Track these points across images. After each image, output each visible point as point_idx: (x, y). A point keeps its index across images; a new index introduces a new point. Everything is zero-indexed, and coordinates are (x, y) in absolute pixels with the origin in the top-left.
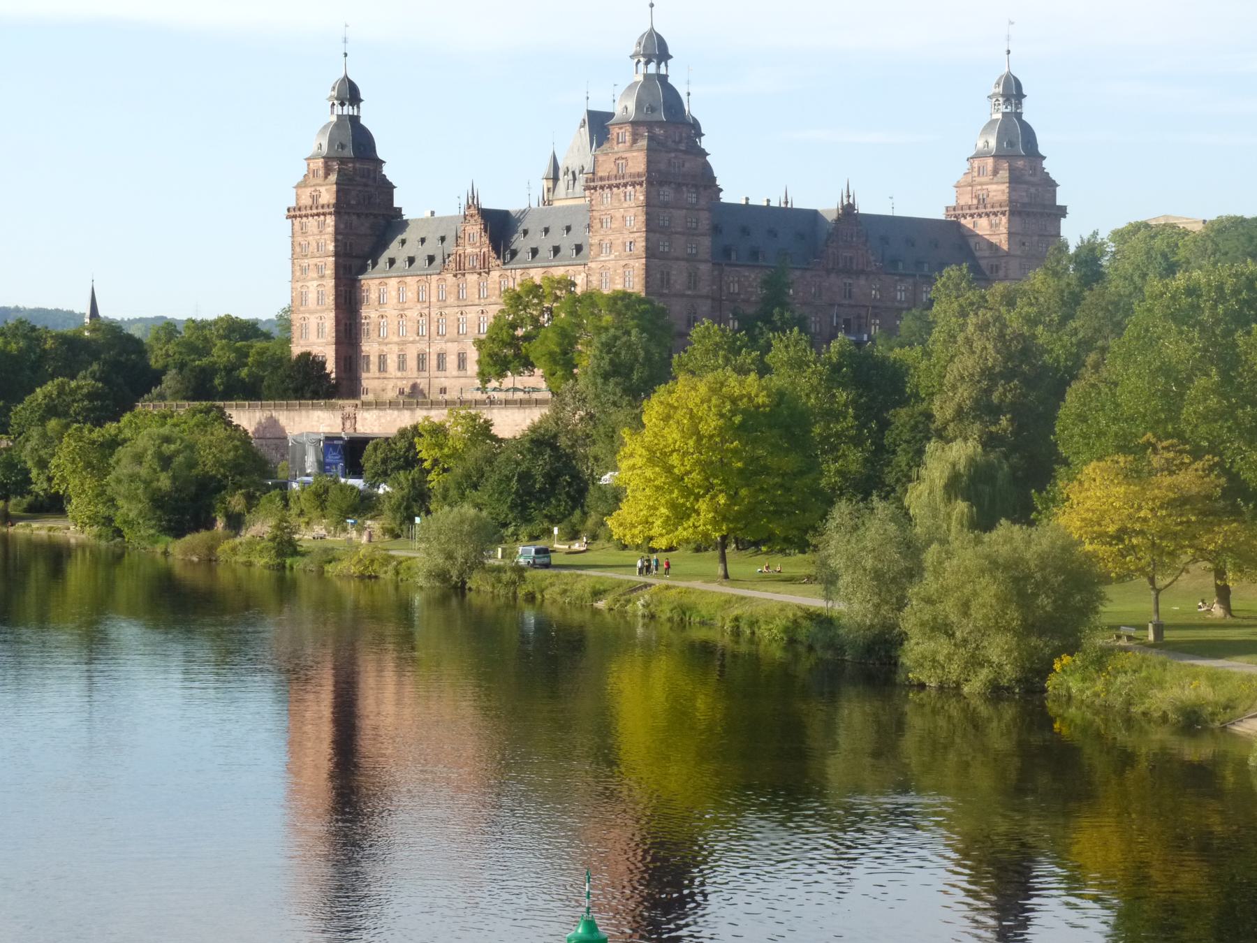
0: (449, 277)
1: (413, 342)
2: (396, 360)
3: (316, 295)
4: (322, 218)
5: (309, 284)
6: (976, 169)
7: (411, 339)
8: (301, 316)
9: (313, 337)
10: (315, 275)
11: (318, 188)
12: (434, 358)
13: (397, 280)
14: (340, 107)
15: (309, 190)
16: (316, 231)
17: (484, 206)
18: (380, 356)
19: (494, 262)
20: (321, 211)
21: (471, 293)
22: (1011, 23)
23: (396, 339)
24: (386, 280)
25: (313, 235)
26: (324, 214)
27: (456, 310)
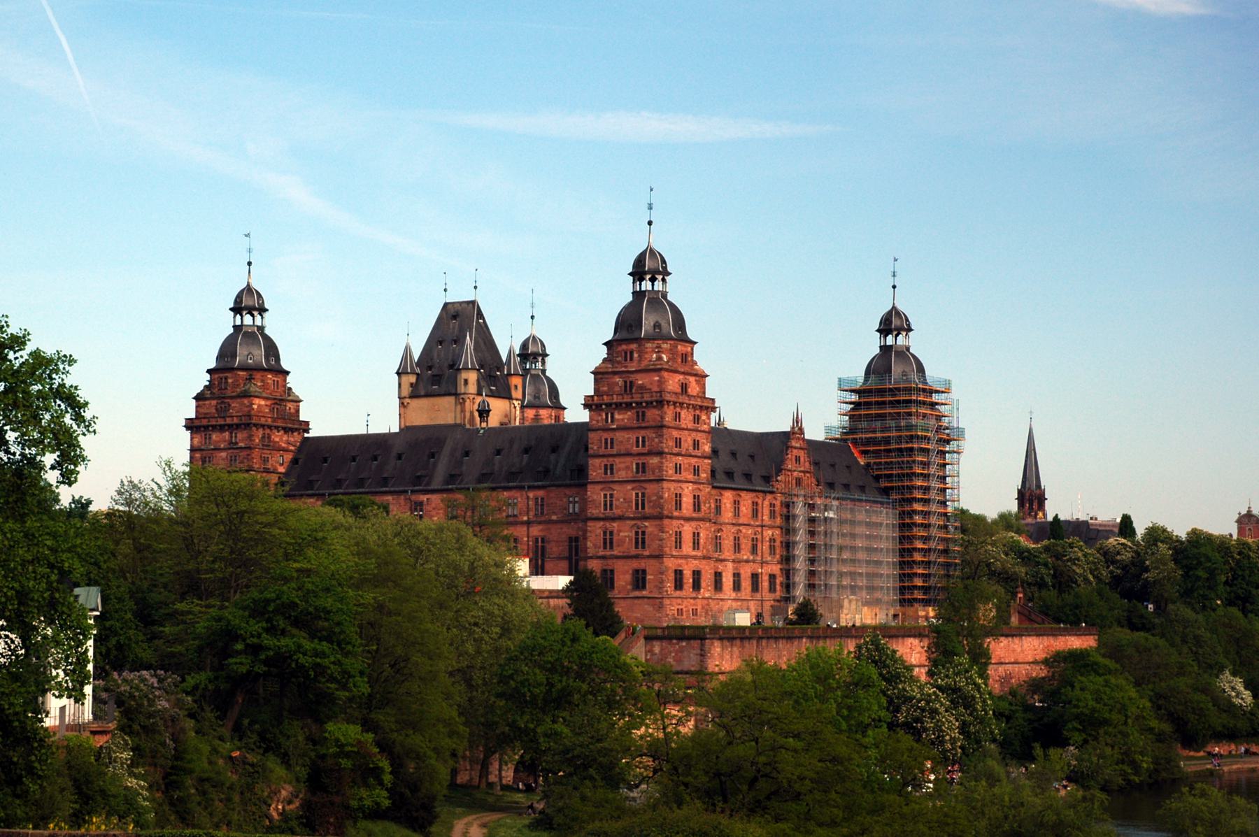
1: (747, 561)
2: (731, 579)
3: (691, 500)
5: (684, 485)
6: (553, 417)
7: (745, 557)
8: (675, 522)
9: (687, 548)
11: (688, 377)
12: (766, 578)
13: (734, 493)
14: (649, 284)
17: (732, 424)
18: (716, 573)
19: (817, 490)
20: (686, 400)
24: (723, 492)
25: (687, 429)
26: (701, 407)
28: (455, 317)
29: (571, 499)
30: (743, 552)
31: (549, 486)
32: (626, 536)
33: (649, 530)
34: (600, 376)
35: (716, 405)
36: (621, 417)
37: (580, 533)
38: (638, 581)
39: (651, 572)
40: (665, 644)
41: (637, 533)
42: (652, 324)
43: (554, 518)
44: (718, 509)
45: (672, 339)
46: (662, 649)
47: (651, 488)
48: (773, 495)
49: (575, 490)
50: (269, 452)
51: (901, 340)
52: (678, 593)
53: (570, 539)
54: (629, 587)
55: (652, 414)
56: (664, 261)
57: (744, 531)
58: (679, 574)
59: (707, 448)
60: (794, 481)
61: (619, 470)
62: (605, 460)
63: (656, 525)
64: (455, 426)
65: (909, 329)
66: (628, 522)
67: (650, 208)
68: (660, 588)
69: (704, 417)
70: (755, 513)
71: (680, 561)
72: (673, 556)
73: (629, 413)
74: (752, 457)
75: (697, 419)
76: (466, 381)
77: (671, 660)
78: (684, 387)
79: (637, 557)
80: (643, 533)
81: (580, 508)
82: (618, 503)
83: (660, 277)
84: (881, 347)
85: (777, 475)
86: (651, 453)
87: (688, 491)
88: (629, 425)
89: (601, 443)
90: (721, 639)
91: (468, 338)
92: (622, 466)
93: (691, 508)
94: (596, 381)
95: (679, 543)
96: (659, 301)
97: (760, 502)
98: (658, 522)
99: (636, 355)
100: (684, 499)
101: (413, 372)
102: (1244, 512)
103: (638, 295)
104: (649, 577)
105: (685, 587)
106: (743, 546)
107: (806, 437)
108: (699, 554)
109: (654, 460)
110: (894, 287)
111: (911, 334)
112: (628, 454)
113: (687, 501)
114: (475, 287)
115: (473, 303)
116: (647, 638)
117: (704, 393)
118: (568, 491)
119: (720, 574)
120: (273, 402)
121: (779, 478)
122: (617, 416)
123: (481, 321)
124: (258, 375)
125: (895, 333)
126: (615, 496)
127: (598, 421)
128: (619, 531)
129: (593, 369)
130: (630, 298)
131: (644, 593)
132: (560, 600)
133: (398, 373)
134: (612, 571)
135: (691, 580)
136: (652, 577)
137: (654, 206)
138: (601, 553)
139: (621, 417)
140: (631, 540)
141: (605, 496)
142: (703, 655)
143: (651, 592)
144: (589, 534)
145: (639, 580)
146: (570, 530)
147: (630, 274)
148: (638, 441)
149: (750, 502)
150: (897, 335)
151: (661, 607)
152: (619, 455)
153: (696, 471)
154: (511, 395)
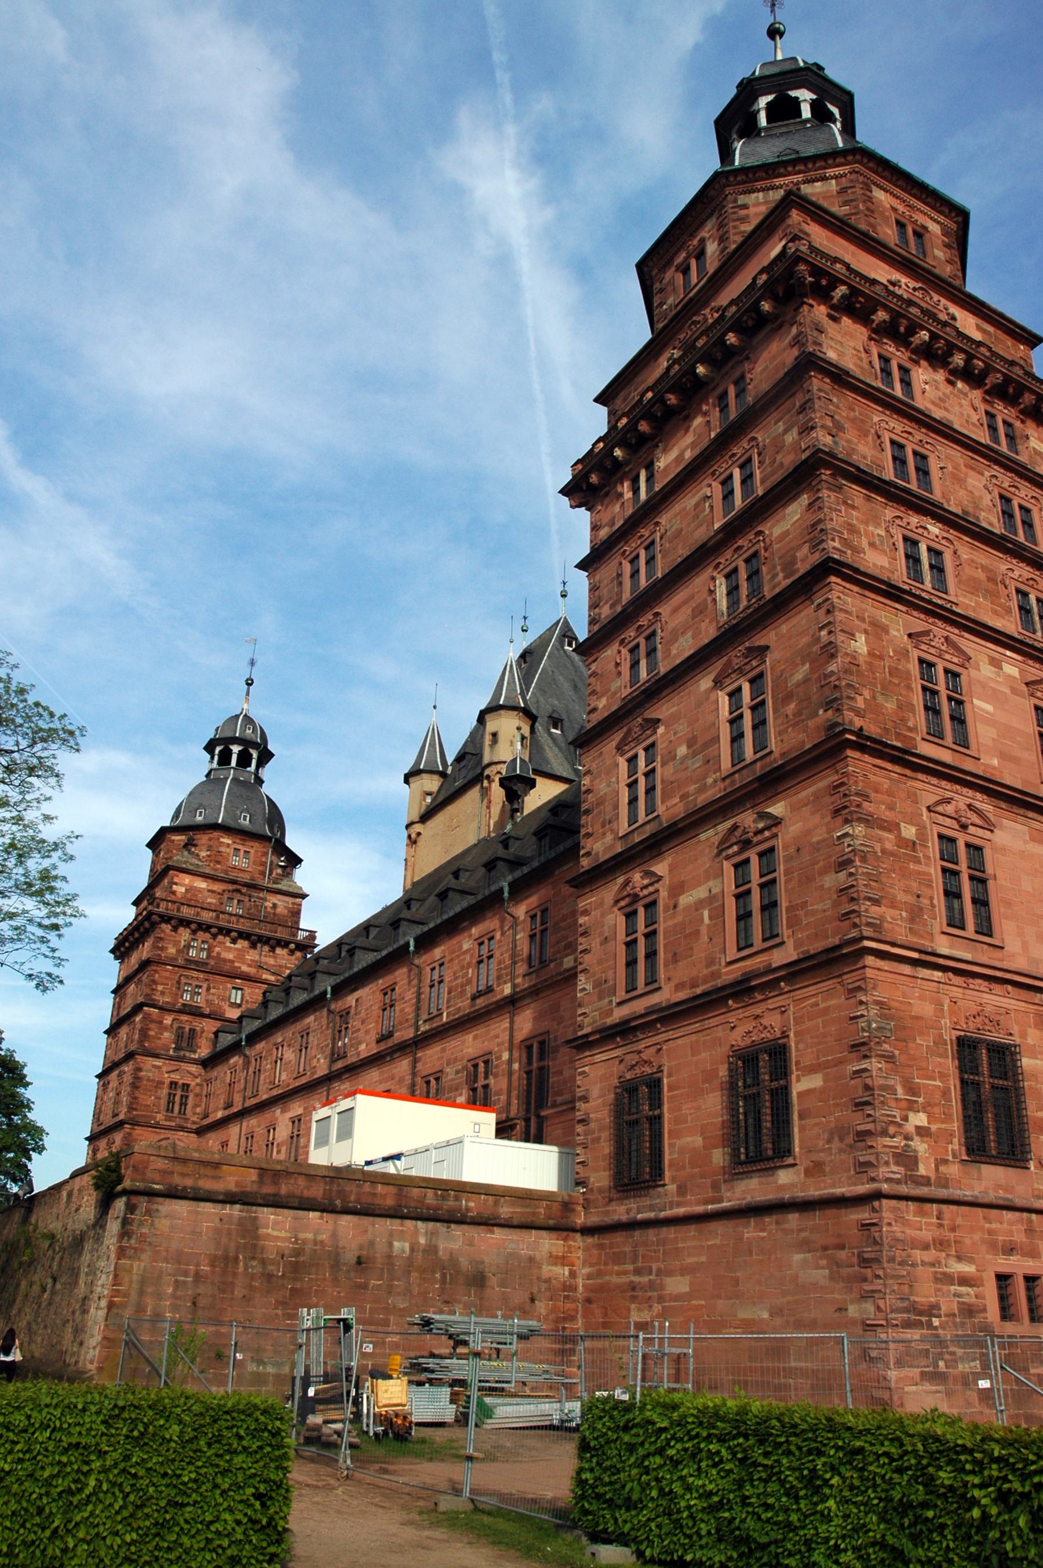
32: (700, 904)
36: (673, 454)
39: (808, 1060)
50: (201, 976)
54: (719, 1157)
63: (817, 797)
66: (711, 835)
68: (862, 1136)
72: (928, 961)
73: (698, 421)
89: (620, 584)
104: (801, 1085)
120: (231, 887)
124: (203, 839)
126: (661, 746)
128: (678, 889)
132: (346, 1221)
134: (654, 1085)
136: (814, 1082)
140: (718, 914)
143: (815, 1170)
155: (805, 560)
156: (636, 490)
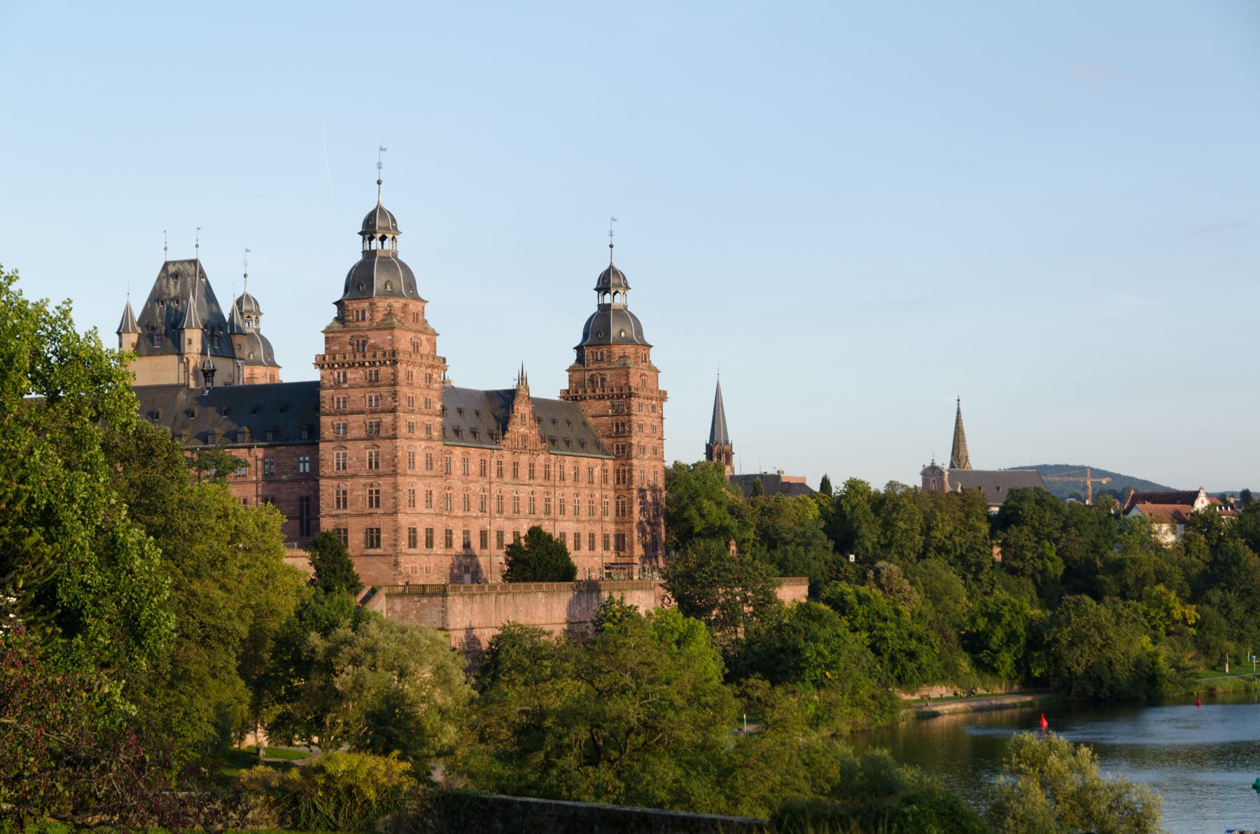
0: (507, 457)
2: (462, 536)
4: (429, 371)
5: (417, 443)
7: (474, 515)
8: (408, 480)
9: (421, 506)
10: (423, 435)
11: (419, 335)
12: (494, 535)
15: (410, 335)
16: (423, 384)
17: (458, 383)
19: (540, 446)
21: (524, 472)
22: (248, 251)
23: (460, 513)
27: (511, 488)
28: (176, 276)
29: (301, 459)
30: (472, 509)
31: (279, 445)
33: (382, 489)
34: (331, 335)
35: (447, 363)
37: (311, 493)
38: (372, 540)
40: (406, 601)
41: (371, 492)
42: (383, 283)
43: (284, 477)
44: (448, 465)
45: (403, 296)
46: (403, 607)
47: (385, 446)
48: (500, 452)
49: (305, 449)
51: (619, 301)
52: (412, 551)
53: (301, 499)
54: (363, 546)
55: (385, 371)
56: (394, 220)
57: (473, 488)
58: (413, 531)
59: (438, 407)
60: (520, 439)
61: (353, 429)
62: (337, 418)
64: (184, 385)
65: (627, 288)
66: (362, 481)
67: (380, 168)
69: (435, 376)
70: (483, 473)
71: (414, 519)
74: (477, 414)
75: (429, 378)
76: (190, 342)
77: (413, 618)
78: (416, 346)
79: (370, 514)
80: (377, 492)
81: (310, 467)
82: (350, 462)
83: (390, 236)
84: (599, 305)
85: (504, 434)
86: (383, 411)
87: (420, 449)
88: (361, 384)
90: (462, 595)
91: (191, 297)
92: (356, 425)
93: (424, 466)
94: (327, 338)
95: (412, 503)
96: (391, 263)
97: (488, 459)
98: (391, 480)
99: (367, 314)
100: (417, 458)
101: (134, 331)
102: (928, 464)
103: (369, 255)
104: (382, 536)
105: (419, 544)
106: (472, 504)
107: (532, 395)
108: (431, 511)
109: (387, 419)
110: (611, 246)
111: (628, 292)
112: (362, 412)
113: (420, 460)
114: (197, 246)
115: (195, 262)
116: (388, 595)
117: (435, 351)
118: (297, 450)
119: (450, 532)
121: (506, 436)
122: (349, 375)
123: (203, 280)
125: (613, 291)
127: (329, 381)
128: (353, 490)
129: (323, 328)
130: (359, 257)
131: (379, 551)
133: (119, 333)
134: (346, 530)
135: (424, 538)
137: (383, 165)
138: (334, 512)
139: (353, 376)
141: (338, 455)
142: (444, 612)
144: (321, 493)
145: (373, 538)
146: (301, 490)
147: (360, 233)
148: (371, 400)
149: (479, 459)
150: (617, 292)
151: (396, 564)
152: (352, 413)
153: (428, 429)
154: (234, 353)
155: (391, 433)
156: (339, 376)
